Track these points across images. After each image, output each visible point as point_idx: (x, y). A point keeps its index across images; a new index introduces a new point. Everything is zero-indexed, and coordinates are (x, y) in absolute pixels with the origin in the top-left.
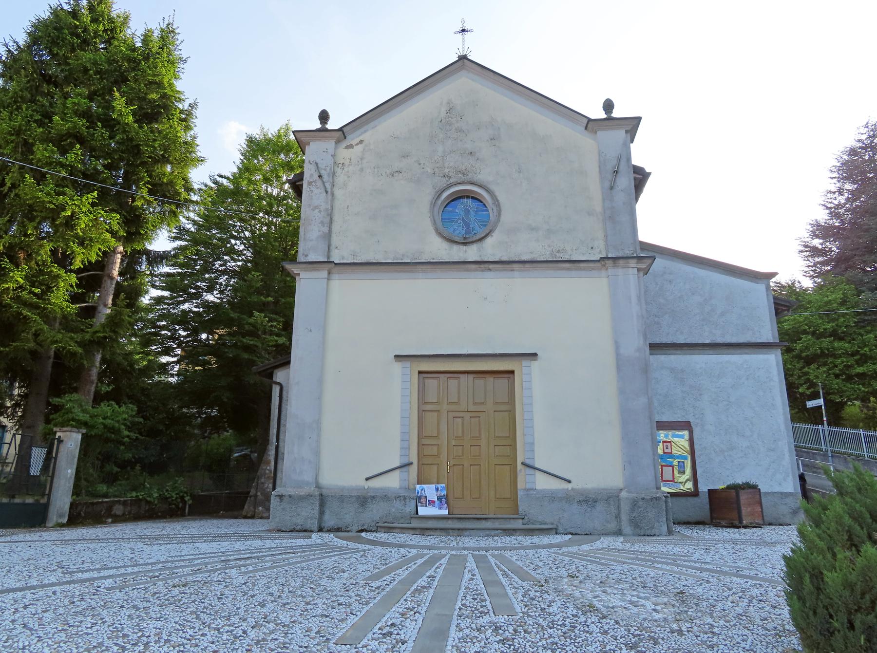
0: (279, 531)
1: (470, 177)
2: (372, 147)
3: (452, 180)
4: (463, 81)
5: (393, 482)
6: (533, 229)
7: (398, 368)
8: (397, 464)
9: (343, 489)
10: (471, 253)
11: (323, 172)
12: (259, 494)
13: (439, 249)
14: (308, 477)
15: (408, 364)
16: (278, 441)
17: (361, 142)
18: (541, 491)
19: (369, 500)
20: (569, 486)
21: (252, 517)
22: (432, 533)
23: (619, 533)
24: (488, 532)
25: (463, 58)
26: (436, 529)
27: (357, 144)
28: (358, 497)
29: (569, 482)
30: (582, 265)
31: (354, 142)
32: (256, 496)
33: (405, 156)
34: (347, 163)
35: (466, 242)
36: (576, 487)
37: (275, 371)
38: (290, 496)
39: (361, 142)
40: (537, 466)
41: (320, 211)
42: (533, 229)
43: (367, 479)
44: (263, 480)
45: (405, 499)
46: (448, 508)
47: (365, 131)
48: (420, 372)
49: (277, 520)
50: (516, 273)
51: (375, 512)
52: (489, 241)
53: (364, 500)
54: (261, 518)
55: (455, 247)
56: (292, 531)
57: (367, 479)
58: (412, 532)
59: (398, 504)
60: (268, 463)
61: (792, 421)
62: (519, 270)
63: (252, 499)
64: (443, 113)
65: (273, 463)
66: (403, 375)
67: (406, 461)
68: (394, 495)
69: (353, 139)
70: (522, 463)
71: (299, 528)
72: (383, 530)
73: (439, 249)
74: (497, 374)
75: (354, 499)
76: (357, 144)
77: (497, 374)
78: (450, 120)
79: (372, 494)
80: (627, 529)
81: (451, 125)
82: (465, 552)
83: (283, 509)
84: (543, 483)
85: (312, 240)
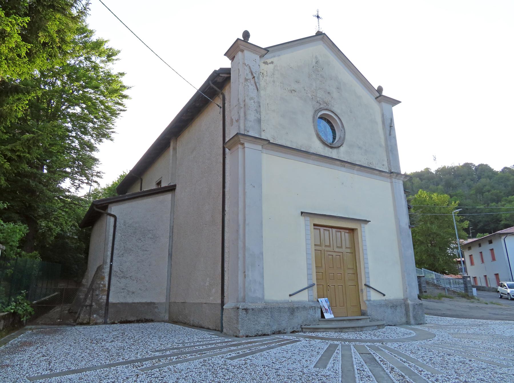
0: (247, 336)
1: (329, 107)
2: (279, 68)
3: (322, 106)
4: (320, 48)
5: (304, 297)
6: (360, 148)
7: (302, 219)
8: (306, 286)
9: (277, 303)
10: (333, 154)
11: (255, 75)
12: (94, 304)
13: (318, 147)
14: (258, 295)
15: (308, 218)
16: (112, 261)
17: (272, 63)
18: (374, 301)
19: (296, 310)
20: (384, 298)
21: (88, 324)
22: (347, 330)
23: (408, 323)
24: (373, 328)
25: (319, 34)
26: (349, 328)
27: (270, 63)
28: (289, 308)
29: (384, 295)
30: (383, 174)
31: (269, 61)
32: (91, 306)
33: (297, 82)
34: (265, 73)
35: (331, 147)
36: (387, 299)
37: (110, 205)
38: (253, 309)
39: (272, 63)
40: (371, 286)
41: (254, 102)
42: (360, 148)
43: (290, 295)
44: (97, 292)
45: (315, 309)
46: (333, 313)
47: (274, 56)
48: (315, 225)
49: (245, 328)
50: (355, 172)
51: (299, 319)
52: (342, 148)
53: (293, 310)
54: (96, 324)
55: (327, 149)
56: (256, 336)
57: (290, 295)
58: (334, 330)
59: (311, 312)
60: (103, 278)
61: (419, 264)
62: (357, 170)
63: (88, 308)
64: (314, 64)
65: (107, 279)
66: (306, 225)
67: (311, 283)
68: (309, 306)
69: (268, 58)
70: (365, 285)
71: (260, 333)
72: (309, 330)
73: (318, 147)
74: (350, 229)
75: (287, 310)
76: (270, 63)
77: (350, 229)
78: (317, 68)
79: (297, 306)
80: (412, 321)
81: (318, 71)
82: (336, 342)
83: (249, 319)
84: (374, 297)
85: (251, 121)
